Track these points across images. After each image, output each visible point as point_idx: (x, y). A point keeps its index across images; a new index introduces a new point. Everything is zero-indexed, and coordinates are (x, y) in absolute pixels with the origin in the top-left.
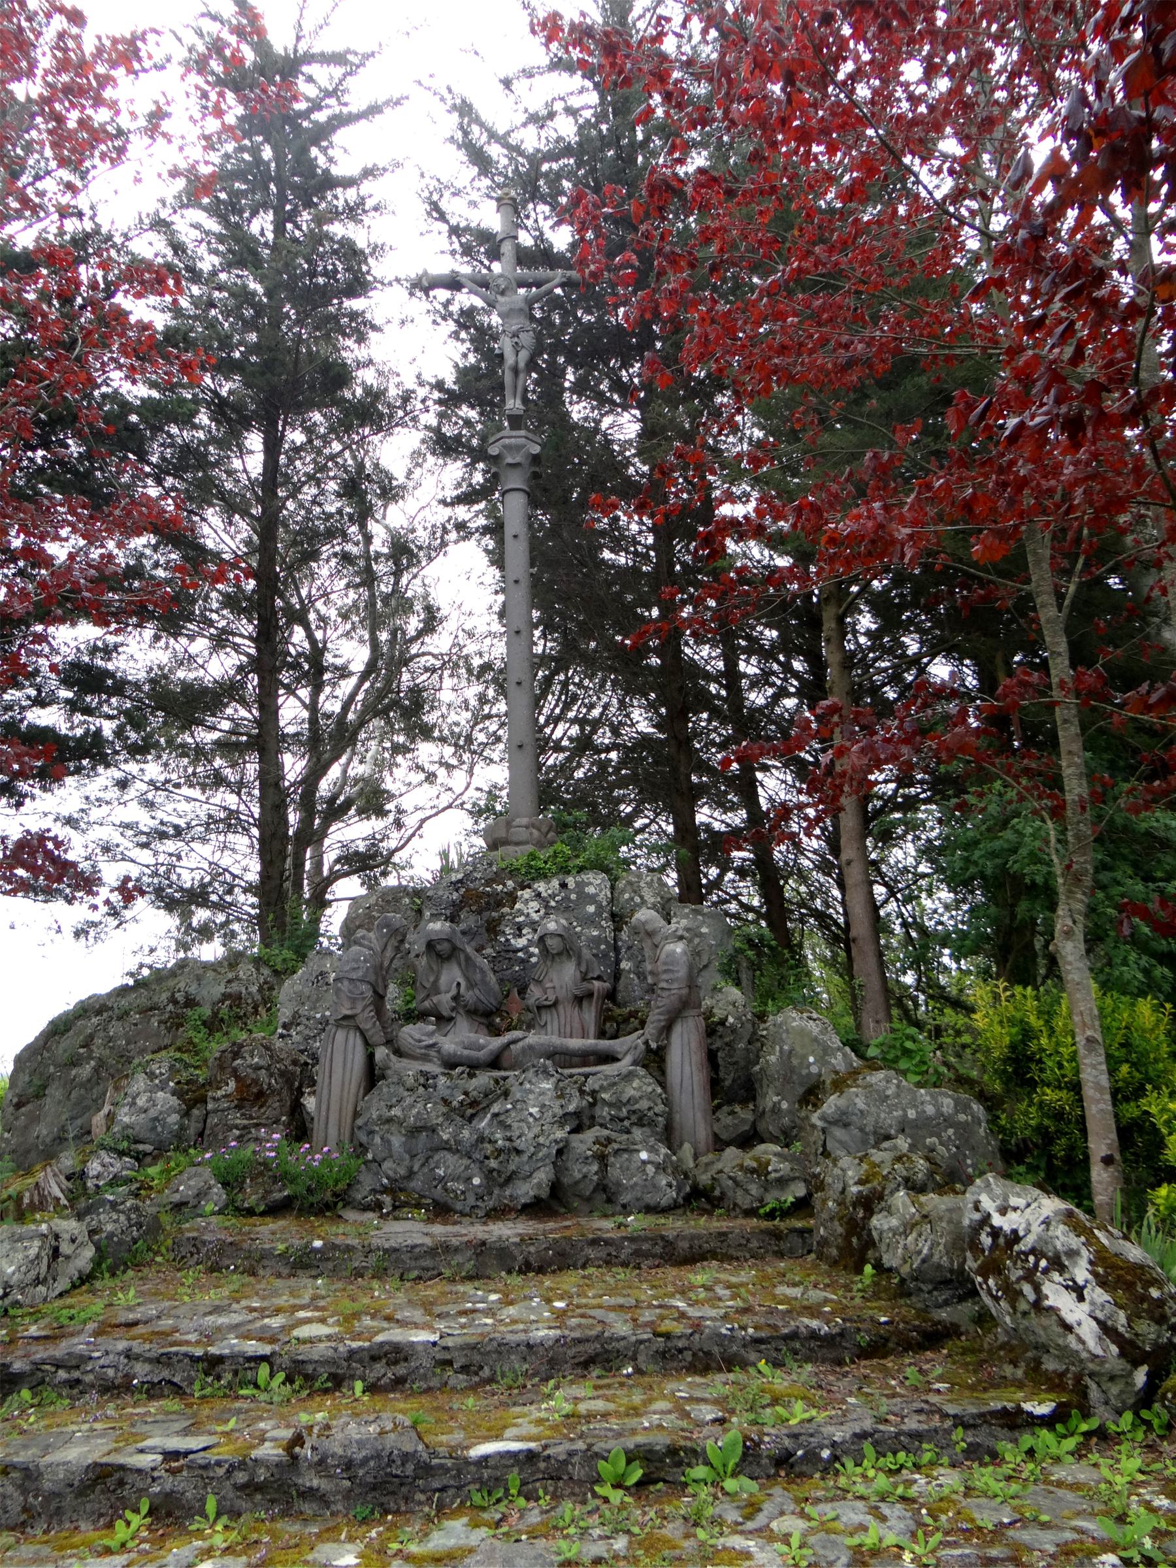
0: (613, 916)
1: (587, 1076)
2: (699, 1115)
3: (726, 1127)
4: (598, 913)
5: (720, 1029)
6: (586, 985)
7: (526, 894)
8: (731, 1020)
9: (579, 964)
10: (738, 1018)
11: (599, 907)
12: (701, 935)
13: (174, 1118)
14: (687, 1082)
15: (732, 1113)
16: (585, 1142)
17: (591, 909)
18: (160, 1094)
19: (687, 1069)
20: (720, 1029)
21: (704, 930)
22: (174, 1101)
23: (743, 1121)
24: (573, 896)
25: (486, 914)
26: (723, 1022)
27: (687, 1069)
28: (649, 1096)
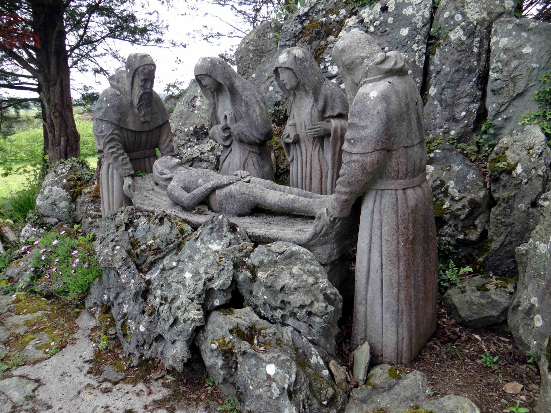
0: (430, 37)
1: (257, 241)
2: (387, 316)
3: (470, 304)
4: (411, 37)
5: (504, 177)
6: (323, 125)
7: (351, 21)
8: (519, 170)
9: (316, 101)
10: (526, 171)
11: (414, 30)
12: (520, 56)
13: (63, 204)
14: (374, 274)
15: (482, 288)
16: (221, 325)
17: (405, 32)
18: (55, 188)
19: (375, 258)
20: (504, 177)
21: (527, 50)
22: (64, 193)
23: (493, 304)
24: (390, 20)
25: (315, 43)
26: (509, 171)
27: (375, 258)
28: (308, 289)
